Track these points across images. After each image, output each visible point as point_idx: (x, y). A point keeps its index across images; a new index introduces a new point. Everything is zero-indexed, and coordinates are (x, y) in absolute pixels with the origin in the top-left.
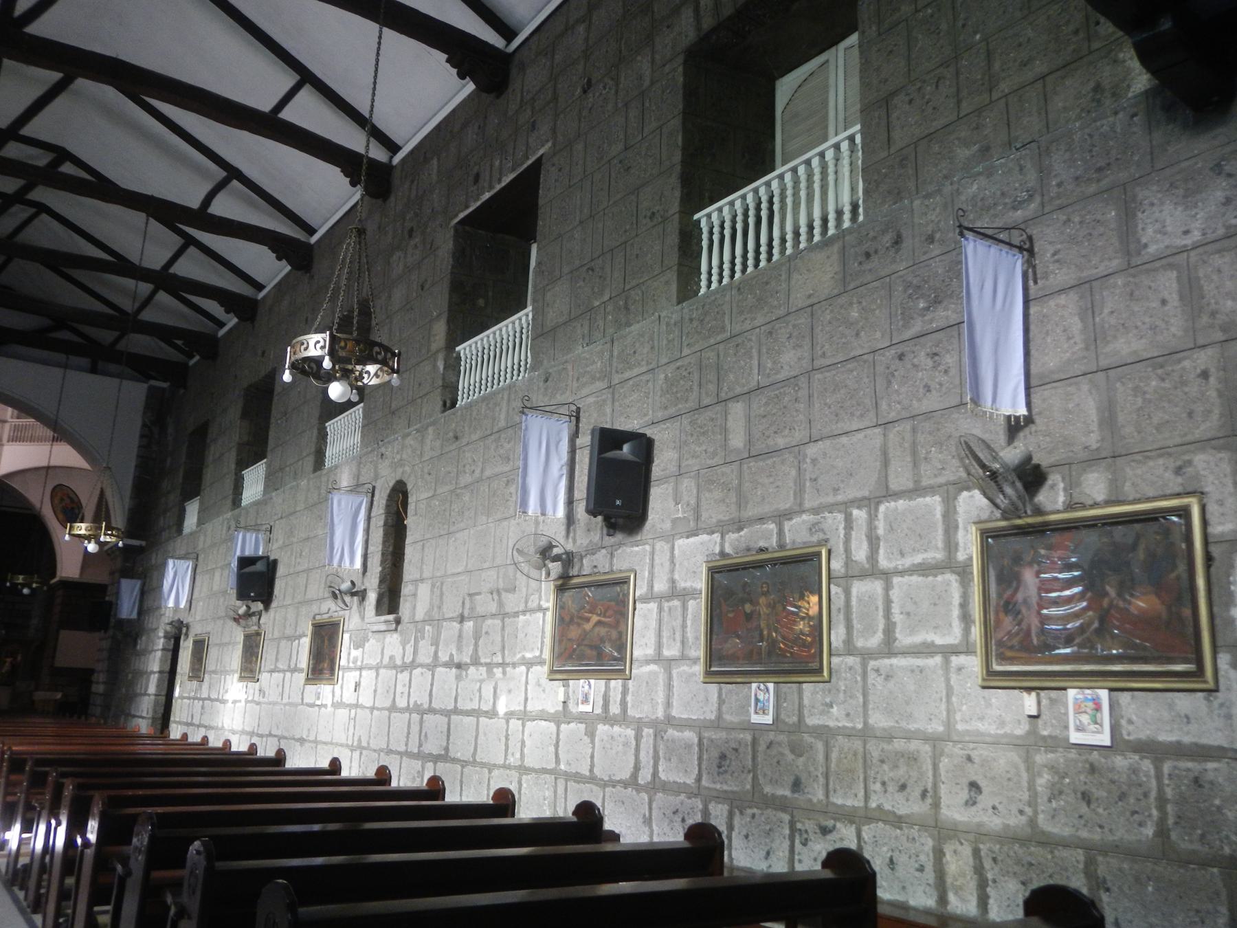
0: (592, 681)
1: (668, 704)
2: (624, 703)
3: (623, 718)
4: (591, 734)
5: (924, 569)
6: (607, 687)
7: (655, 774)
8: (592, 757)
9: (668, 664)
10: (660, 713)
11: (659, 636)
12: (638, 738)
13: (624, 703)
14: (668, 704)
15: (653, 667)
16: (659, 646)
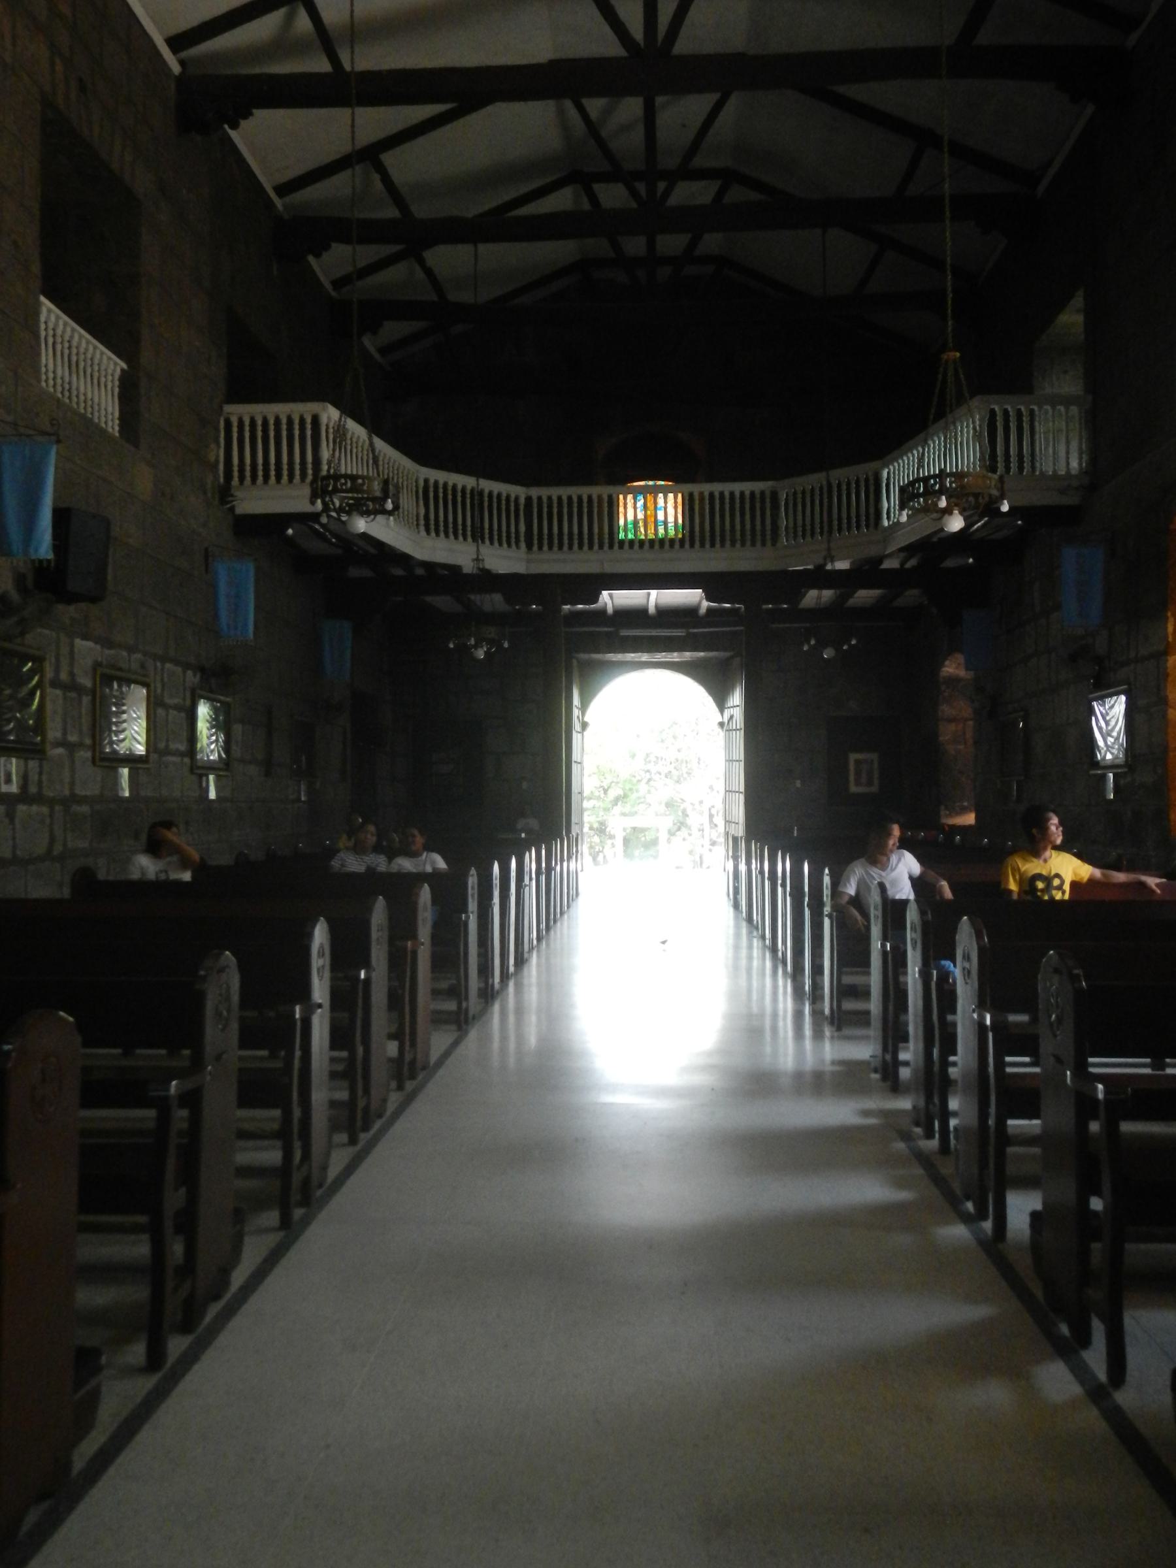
0: (14, 760)
1: (72, 784)
2: (40, 782)
3: (39, 799)
4: (11, 816)
5: (177, 708)
6: (26, 766)
7: (65, 845)
8: (14, 838)
9: (71, 748)
10: (67, 792)
11: (65, 722)
12: (51, 816)
13: (40, 782)
14: (72, 784)
15: (60, 750)
16: (65, 733)
